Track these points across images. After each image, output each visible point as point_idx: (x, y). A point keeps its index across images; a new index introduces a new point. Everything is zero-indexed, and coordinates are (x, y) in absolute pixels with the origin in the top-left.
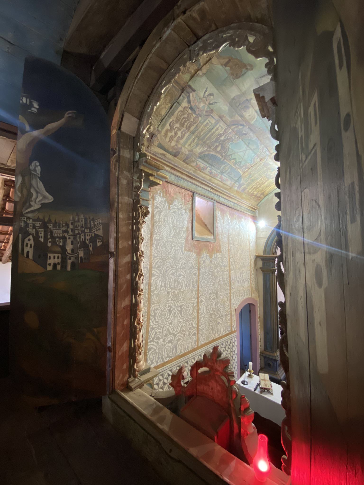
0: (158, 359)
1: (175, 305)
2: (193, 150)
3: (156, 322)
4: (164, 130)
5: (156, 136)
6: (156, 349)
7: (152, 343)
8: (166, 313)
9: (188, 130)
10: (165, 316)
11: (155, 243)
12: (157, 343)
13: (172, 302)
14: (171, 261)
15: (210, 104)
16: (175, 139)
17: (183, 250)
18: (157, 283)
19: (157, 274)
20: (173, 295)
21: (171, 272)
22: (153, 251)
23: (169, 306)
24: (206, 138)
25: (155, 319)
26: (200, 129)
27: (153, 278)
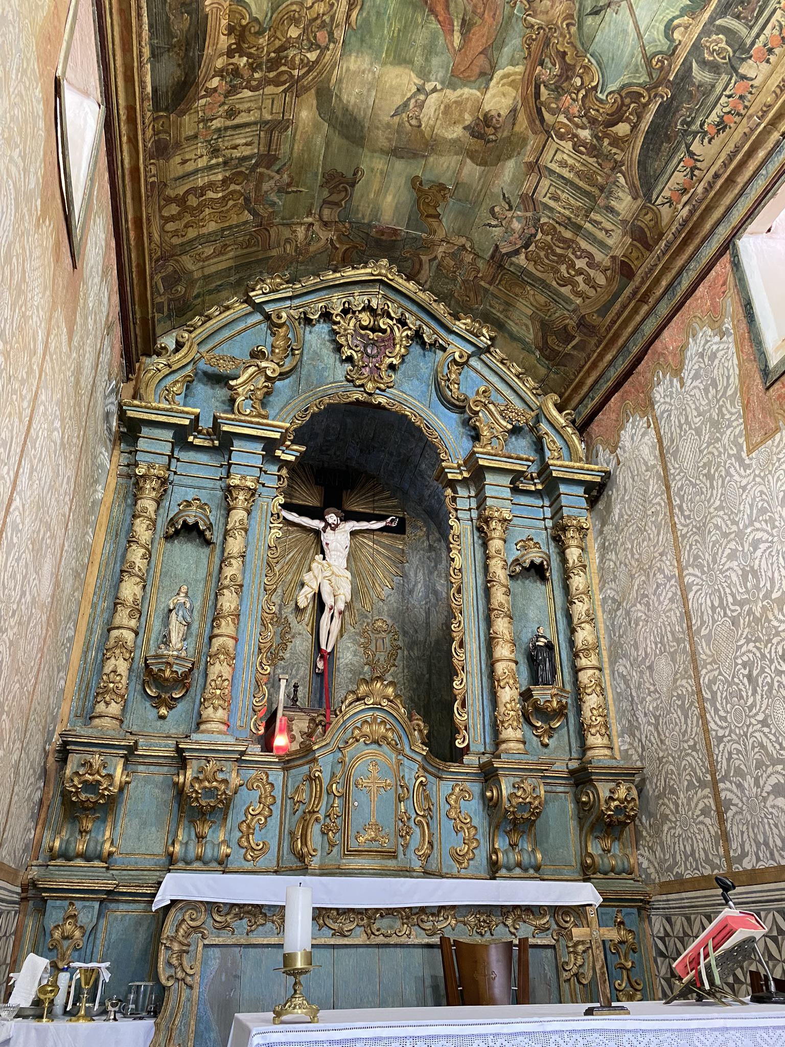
0: (758, 848)
1: (763, 656)
2: (624, 222)
3: (721, 718)
4: (572, 297)
5: (583, 317)
6: (741, 808)
7: (728, 785)
8: (741, 687)
9: (573, 241)
10: (742, 697)
11: (678, 502)
12: (739, 786)
13: (752, 645)
14: (719, 520)
15: (511, 208)
16: (592, 273)
17: (744, 455)
18: (701, 604)
19: (697, 580)
20: (749, 625)
21: (728, 551)
22: (679, 526)
23: (744, 665)
24: (588, 188)
25: (716, 711)
26: (567, 213)
27: (691, 596)
